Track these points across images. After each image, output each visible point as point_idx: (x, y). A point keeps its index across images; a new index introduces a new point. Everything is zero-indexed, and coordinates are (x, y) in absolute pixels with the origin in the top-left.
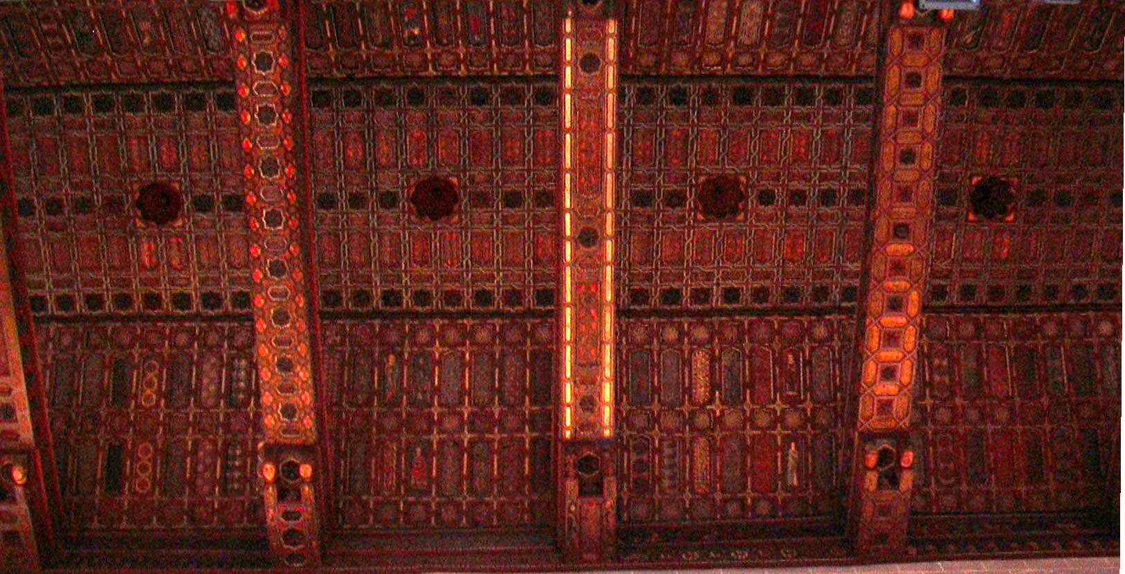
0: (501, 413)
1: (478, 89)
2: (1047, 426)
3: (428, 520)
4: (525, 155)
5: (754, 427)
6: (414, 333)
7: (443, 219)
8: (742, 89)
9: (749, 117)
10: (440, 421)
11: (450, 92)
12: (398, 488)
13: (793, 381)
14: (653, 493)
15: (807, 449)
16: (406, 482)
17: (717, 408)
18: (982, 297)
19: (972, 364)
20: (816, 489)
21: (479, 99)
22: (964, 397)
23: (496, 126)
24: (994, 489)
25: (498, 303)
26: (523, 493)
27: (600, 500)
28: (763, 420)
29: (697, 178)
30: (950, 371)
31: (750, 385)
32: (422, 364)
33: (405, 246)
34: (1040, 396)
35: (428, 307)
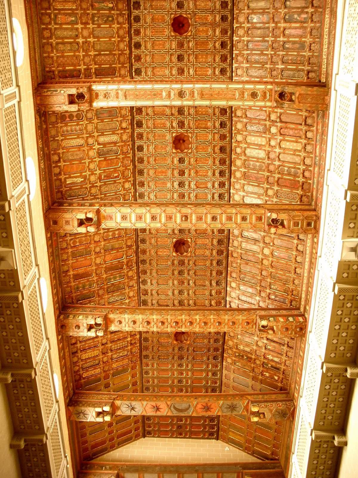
0: (91, 55)
1: (227, 45)
2: (95, 279)
3: (44, 24)
4: (199, 63)
5: (89, 163)
6: (121, 15)
7: (172, 29)
8: (225, 150)
9: (214, 152)
10: (86, 28)
11: (226, 33)
12: (56, 9)
13: (108, 177)
14: (61, 123)
15: (81, 186)
16: (59, 14)
17: (97, 147)
18: (142, 246)
19: (117, 246)
20: (66, 190)
21: (223, 45)
22: (104, 245)
23: (212, 52)
24: (70, 262)
25: (135, 52)
26: (58, 67)
27: (67, 103)
28: (92, 166)
29: (190, 133)
30: (114, 238)
31: (105, 159)
32: (109, 20)
33: (161, 12)
34: (106, 274)
35: (133, 21)
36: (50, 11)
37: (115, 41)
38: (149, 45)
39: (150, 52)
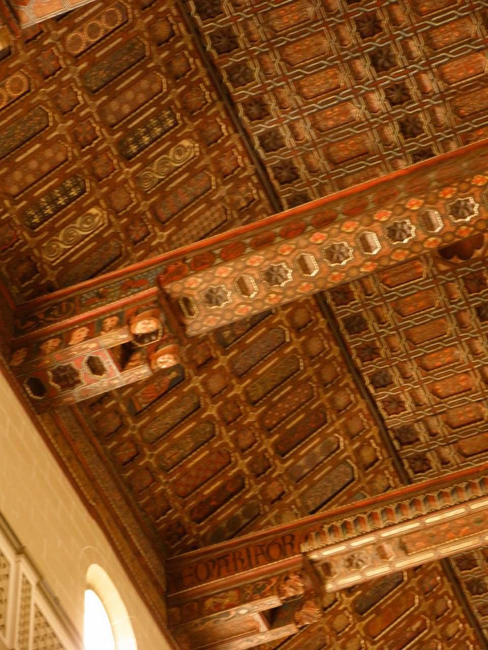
0: (251, 424)
25: (354, 342)
36: (113, 402)
37: (295, 350)
38: (388, 314)
39: (397, 329)
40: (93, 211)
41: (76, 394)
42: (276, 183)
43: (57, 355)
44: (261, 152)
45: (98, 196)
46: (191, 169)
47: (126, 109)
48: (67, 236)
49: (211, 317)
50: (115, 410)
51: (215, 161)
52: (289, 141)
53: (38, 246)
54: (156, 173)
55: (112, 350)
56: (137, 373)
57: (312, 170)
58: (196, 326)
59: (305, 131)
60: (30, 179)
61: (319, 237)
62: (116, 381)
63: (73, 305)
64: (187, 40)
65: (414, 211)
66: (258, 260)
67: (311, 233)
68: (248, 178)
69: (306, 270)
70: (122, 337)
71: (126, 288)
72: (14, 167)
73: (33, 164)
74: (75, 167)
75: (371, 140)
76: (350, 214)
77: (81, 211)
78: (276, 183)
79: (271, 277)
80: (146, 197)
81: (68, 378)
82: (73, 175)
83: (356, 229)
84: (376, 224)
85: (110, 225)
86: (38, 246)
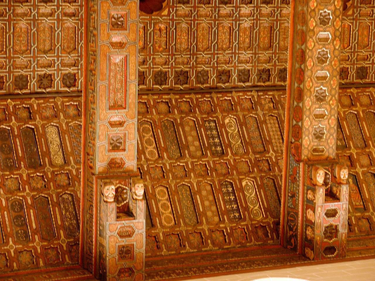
37: (363, 111)
38: (364, 53)
40: (244, 184)
41: (343, 231)
42: (267, 83)
43: (317, 232)
44: (247, 84)
45: (237, 178)
46: (242, 124)
47: (197, 143)
48: (252, 203)
49: (329, 141)
50: (358, 219)
51: (243, 110)
52: (248, 67)
53: (251, 220)
54: (236, 143)
55: (326, 201)
56: (344, 192)
57: (269, 60)
58: (331, 151)
59: (246, 55)
60: (214, 208)
61: (309, 63)
62: (344, 206)
63: (292, 215)
64: (173, 97)
65: (317, 6)
66: (308, 101)
67: (306, 66)
68: (259, 96)
69: (325, 78)
70: (321, 192)
71: (294, 180)
72: (204, 214)
73: (207, 203)
74: (216, 182)
75: (265, 23)
76: (304, 41)
77: (242, 189)
78: (267, 83)
79: (320, 99)
80: (247, 153)
81: (331, 231)
82: (221, 185)
83: (313, 41)
84: (315, 30)
85: (255, 178)
86: (251, 220)
